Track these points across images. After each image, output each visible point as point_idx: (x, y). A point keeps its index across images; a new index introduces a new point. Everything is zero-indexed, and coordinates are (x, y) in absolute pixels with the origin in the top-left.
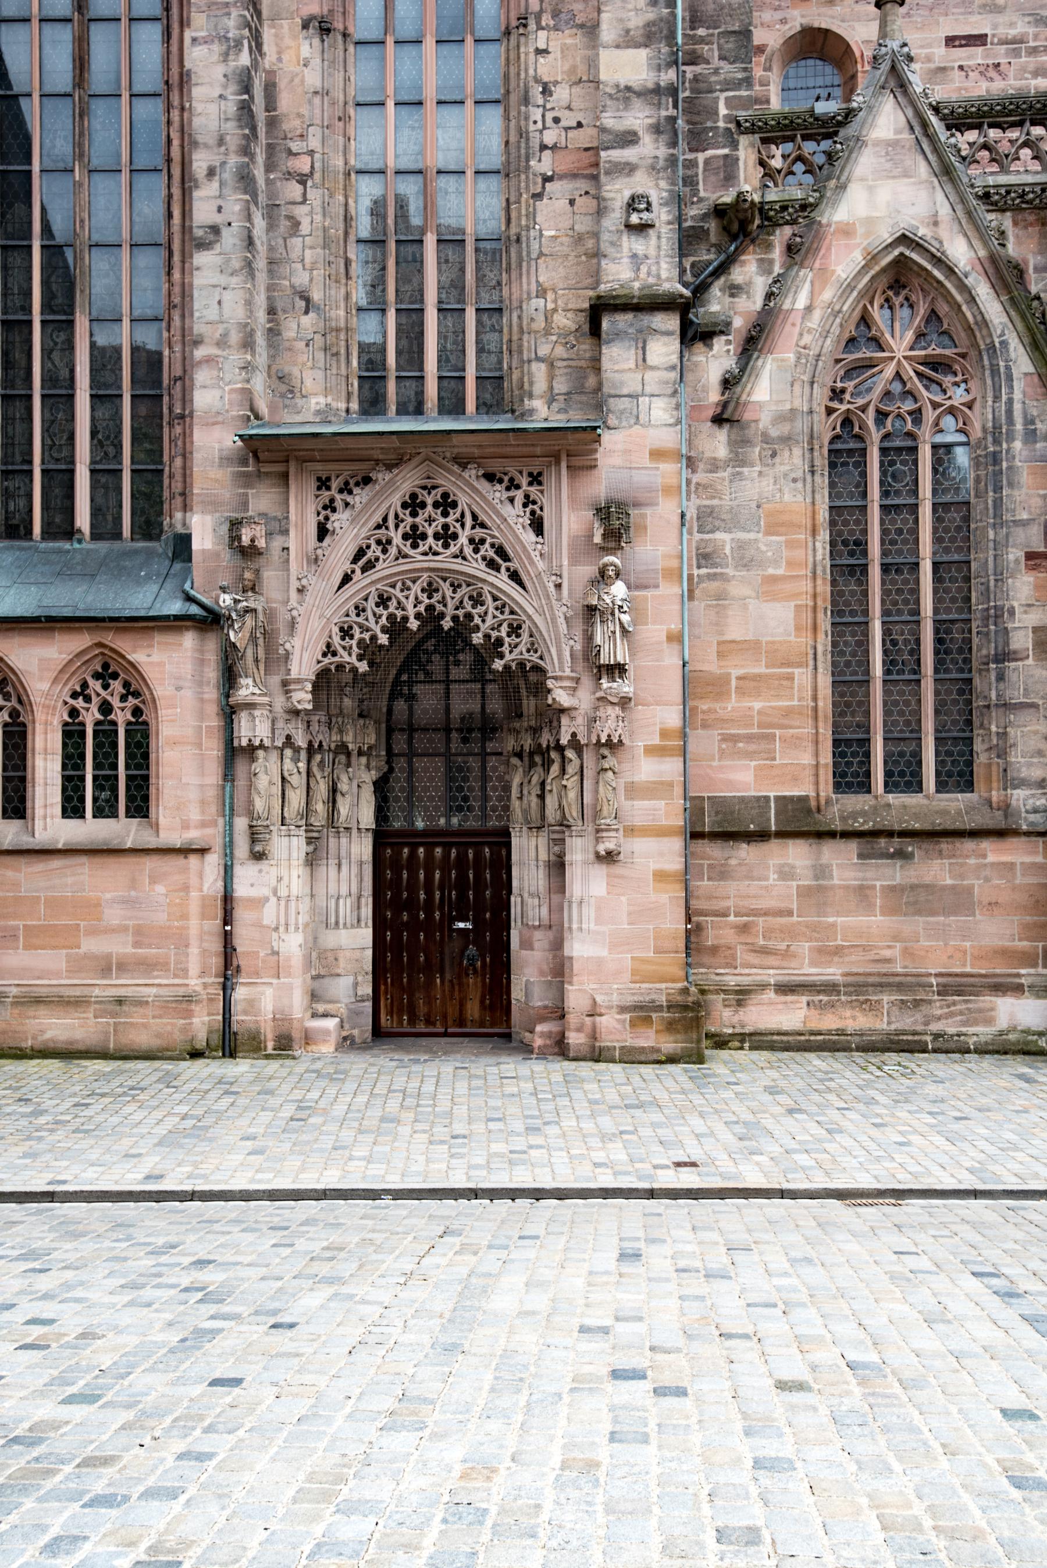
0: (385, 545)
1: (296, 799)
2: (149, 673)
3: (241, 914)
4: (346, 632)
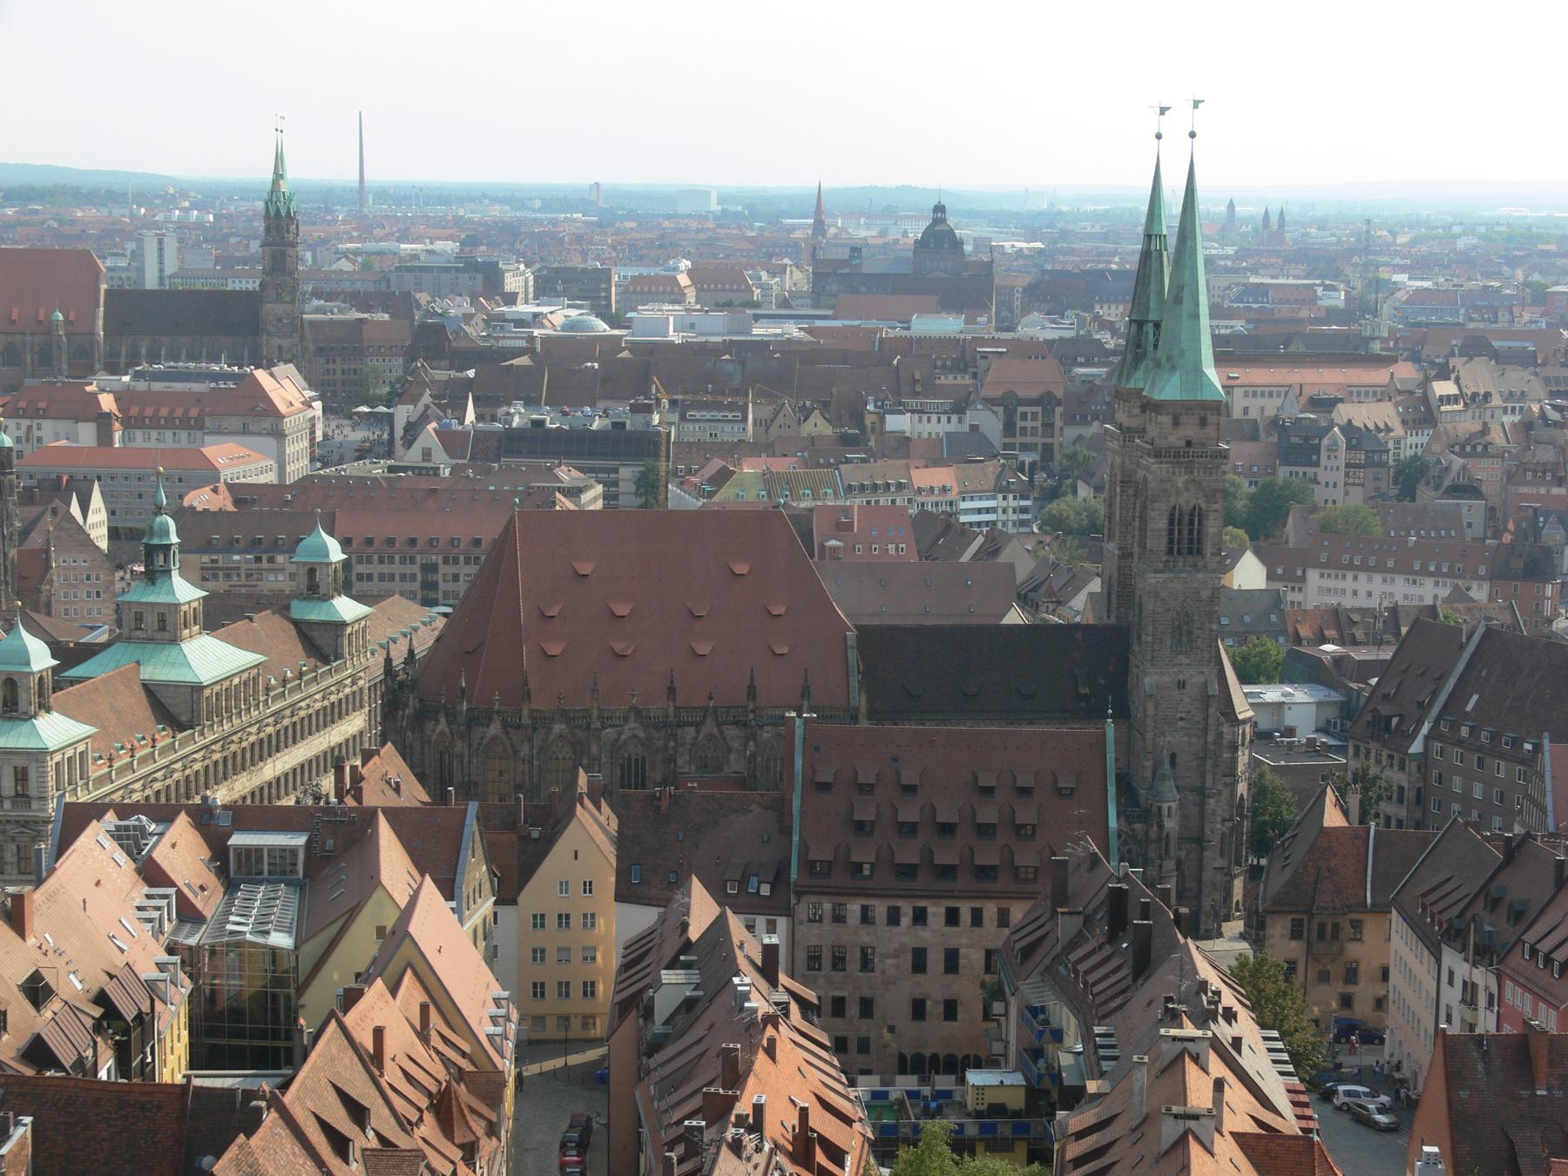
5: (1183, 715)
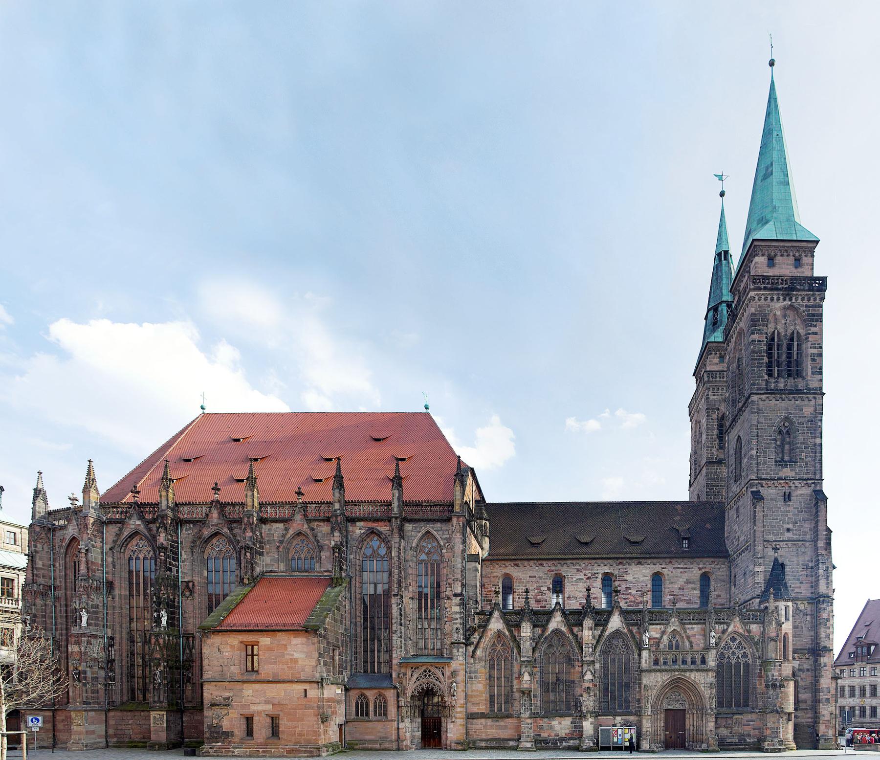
0: (421, 677)
1: (408, 714)
2: (387, 696)
3: (400, 730)
4: (415, 690)
5: (790, 526)
